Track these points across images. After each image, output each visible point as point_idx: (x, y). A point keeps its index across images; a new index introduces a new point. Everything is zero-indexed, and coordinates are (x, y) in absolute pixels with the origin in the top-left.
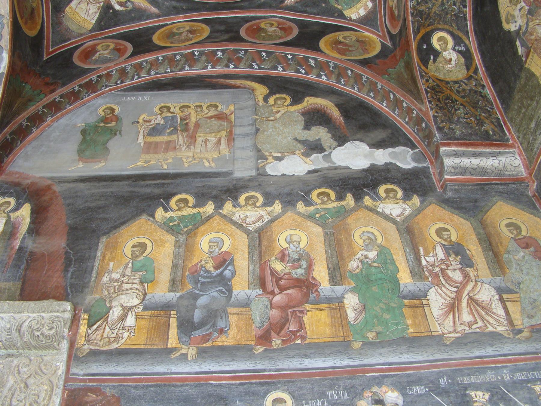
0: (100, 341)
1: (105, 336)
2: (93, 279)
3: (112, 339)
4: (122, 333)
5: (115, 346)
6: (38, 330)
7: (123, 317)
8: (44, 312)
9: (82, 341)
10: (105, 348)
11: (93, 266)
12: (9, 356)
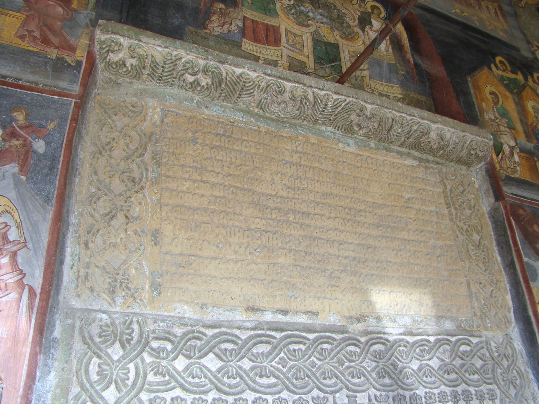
2: (479, 114)
6: (474, 150)
7: (512, 154)
8: (479, 136)
11: (473, 102)
12: (437, 163)
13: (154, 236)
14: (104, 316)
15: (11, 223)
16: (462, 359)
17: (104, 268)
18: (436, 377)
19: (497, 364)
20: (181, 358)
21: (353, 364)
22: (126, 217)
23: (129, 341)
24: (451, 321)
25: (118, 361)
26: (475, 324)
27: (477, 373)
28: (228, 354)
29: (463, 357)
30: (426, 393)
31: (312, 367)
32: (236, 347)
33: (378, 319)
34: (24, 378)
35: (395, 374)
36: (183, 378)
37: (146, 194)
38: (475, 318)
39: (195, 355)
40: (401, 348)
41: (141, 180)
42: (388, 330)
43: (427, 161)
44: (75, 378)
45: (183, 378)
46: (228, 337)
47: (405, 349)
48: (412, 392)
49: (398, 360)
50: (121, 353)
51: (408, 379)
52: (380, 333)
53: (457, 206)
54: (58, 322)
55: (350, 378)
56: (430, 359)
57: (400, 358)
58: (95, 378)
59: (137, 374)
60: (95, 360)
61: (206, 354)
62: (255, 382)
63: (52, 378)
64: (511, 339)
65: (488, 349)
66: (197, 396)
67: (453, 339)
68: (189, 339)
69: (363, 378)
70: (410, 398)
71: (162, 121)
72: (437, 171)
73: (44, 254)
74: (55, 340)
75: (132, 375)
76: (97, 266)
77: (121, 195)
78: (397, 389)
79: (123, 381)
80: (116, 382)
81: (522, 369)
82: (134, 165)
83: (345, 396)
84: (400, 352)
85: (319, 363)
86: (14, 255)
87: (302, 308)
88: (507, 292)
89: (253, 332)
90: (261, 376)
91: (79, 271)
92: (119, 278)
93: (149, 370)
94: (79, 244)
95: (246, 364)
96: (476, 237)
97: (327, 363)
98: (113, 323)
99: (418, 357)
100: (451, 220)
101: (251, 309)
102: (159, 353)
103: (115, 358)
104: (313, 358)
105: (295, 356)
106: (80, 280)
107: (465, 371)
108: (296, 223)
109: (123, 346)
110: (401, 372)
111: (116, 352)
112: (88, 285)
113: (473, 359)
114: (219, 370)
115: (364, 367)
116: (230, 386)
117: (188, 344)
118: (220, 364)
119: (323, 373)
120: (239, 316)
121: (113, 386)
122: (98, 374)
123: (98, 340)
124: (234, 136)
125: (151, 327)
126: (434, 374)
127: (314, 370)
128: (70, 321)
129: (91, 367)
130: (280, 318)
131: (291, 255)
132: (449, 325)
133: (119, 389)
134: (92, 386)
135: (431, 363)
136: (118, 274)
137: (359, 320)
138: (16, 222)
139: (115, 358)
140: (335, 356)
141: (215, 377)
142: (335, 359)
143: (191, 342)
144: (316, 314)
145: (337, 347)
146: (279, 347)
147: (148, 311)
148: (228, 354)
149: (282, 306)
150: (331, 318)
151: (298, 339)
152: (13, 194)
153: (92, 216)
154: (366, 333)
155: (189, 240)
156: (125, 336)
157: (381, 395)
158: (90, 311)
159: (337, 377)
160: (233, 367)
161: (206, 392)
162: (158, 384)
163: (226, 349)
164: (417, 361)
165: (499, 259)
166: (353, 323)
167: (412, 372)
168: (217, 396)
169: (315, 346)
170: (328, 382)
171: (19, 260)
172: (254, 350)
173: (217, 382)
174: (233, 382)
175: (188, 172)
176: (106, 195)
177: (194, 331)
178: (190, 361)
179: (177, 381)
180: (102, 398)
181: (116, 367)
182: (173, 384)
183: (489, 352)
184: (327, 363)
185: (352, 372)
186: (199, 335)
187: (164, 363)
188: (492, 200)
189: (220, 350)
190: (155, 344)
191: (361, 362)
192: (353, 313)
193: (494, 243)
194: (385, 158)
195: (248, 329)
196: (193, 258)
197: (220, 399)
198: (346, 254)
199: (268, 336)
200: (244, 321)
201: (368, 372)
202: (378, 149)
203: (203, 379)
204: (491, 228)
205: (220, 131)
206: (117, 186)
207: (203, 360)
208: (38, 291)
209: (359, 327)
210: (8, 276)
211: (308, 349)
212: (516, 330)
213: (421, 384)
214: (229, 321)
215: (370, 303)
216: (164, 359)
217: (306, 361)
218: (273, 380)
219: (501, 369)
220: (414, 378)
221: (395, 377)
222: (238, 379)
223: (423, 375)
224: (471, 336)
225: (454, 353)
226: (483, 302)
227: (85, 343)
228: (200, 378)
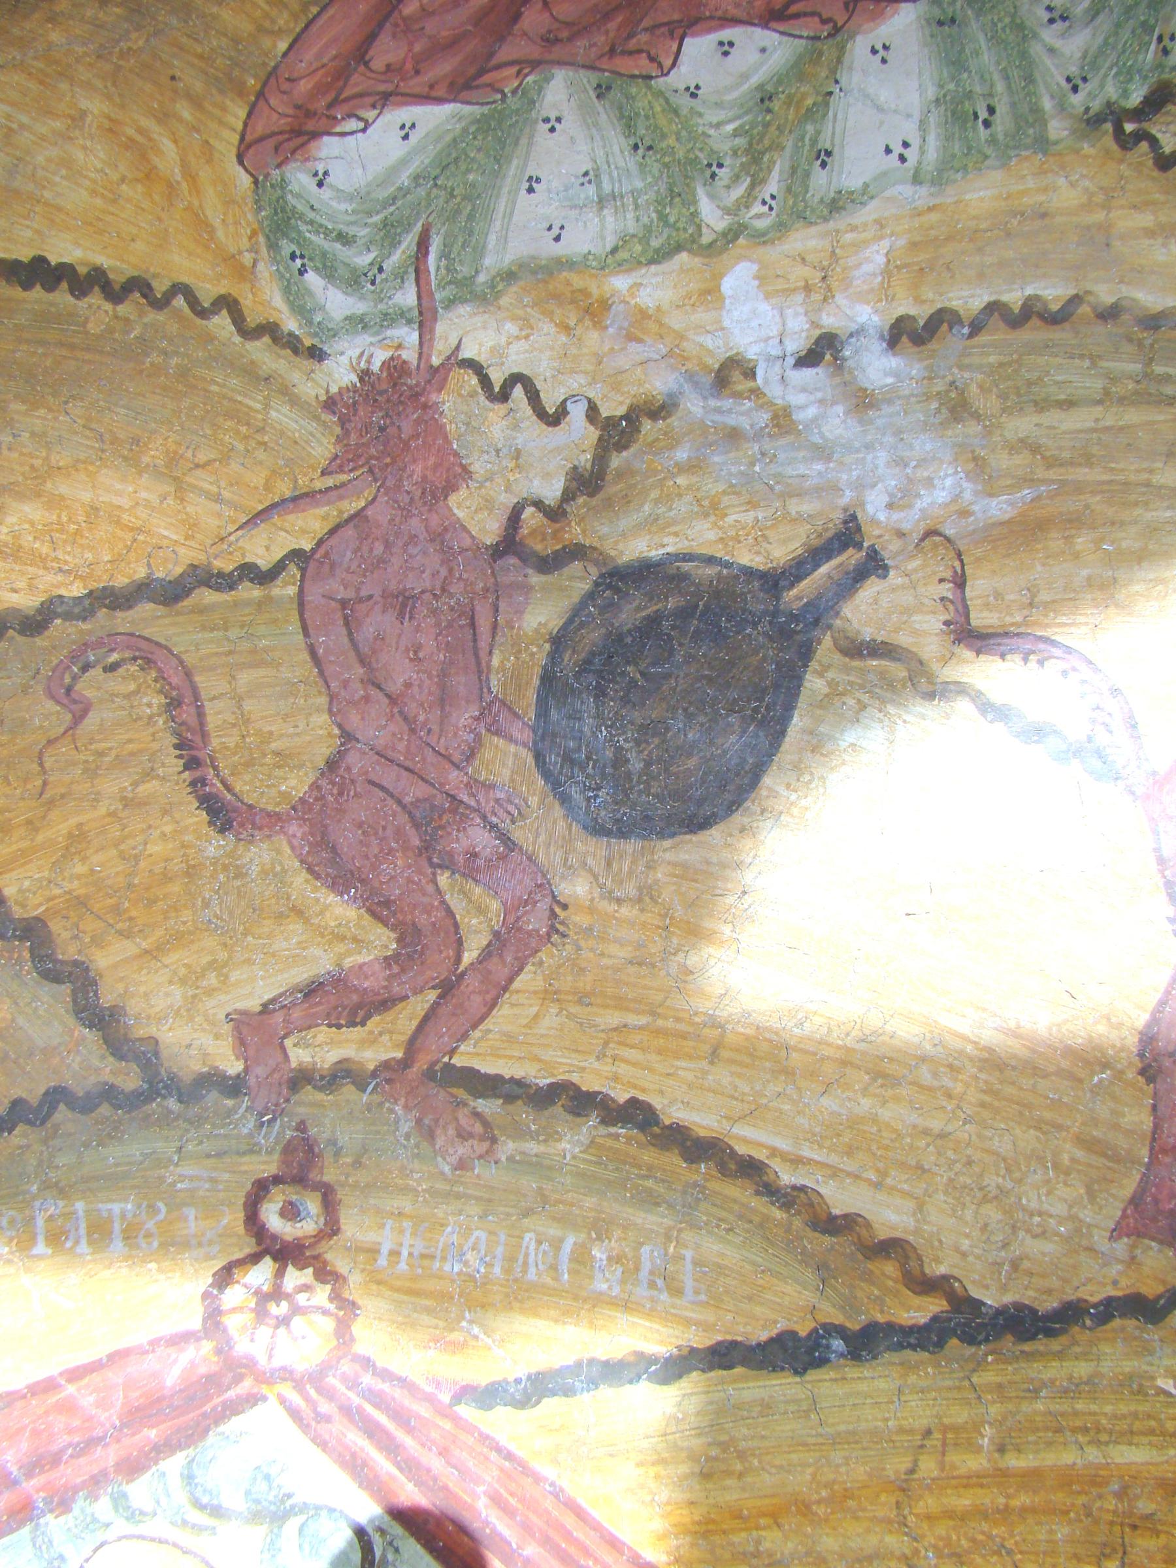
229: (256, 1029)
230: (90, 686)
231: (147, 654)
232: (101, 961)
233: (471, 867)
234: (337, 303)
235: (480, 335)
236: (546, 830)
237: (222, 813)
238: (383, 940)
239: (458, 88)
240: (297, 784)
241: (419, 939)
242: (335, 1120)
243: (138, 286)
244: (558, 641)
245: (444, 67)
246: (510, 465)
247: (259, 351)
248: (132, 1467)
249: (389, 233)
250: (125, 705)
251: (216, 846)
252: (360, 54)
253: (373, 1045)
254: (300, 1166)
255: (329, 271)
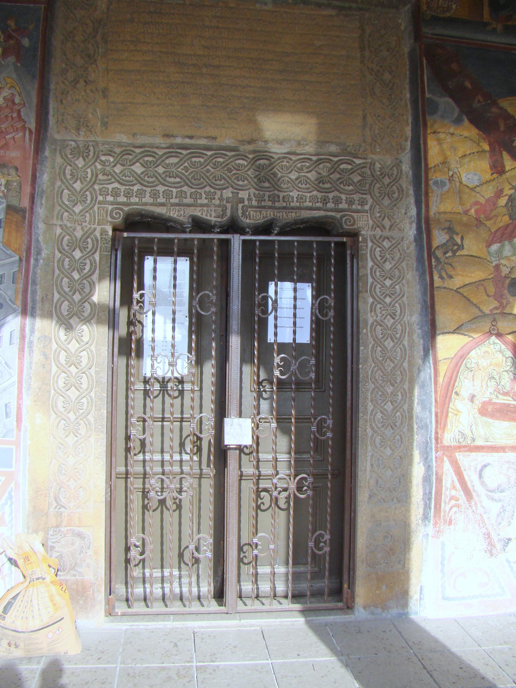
0: (437, 9)
1: (440, 5)
3: (445, 9)
4: (452, 5)
5: (448, 15)
9: (424, 7)
10: (442, 16)
13: (103, 92)
14: (73, 143)
15: (16, 93)
16: (340, 174)
17: (73, 115)
18: (310, 185)
19: (377, 180)
20: (119, 166)
21: (239, 172)
22: (85, 81)
23: (87, 156)
24: (337, 145)
25: (82, 168)
26: (362, 149)
27: (352, 185)
28: (148, 163)
29: (342, 172)
30: (298, 195)
31: (207, 173)
32: (154, 160)
33: (266, 142)
34: (30, 176)
35: (274, 180)
36: (119, 177)
37: (99, 65)
38: (363, 144)
39: (127, 164)
40: (284, 164)
41: (94, 55)
42: (273, 150)
43: (350, 9)
44: (58, 177)
45: (119, 177)
46: (150, 153)
47: (288, 164)
48: (286, 194)
49: (279, 171)
50: (83, 163)
51: (284, 184)
52: (266, 152)
53: (373, 49)
54: (47, 147)
55: (235, 181)
56: (307, 172)
57: (281, 170)
58: (69, 177)
59: (92, 175)
60: (69, 167)
61: (134, 163)
62: (165, 180)
63: (46, 177)
64: (401, 162)
65: (370, 168)
66: (127, 187)
67: (336, 159)
68: (124, 155)
69: (246, 182)
70: (283, 197)
71: (108, 9)
72: (358, 17)
73: (35, 109)
74: (46, 157)
75: (89, 176)
76: (68, 114)
77: (81, 67)
78: (274, 191)
79: (84, 178)
80: (80, 179)
81: (404, 186)
82: (90, 45)
83: (230, 192)
84: (282, 166)
85: (213, 170)
86: (19, 111)
87: (205, 135)
88: (408, 124)
89: (167, 150)
90: (170, 177)
91: (58, 118)
92: (82, 120)
93: (99, 172)
94: (57, 102)
95: (161, 170)
96: (387, 76)
97: (219, 171)
98: (78, 147)
99: (297, 170)
100: (362, 62)
101: (167, 136)
102: (105, 163)
103: (80, 166)
104: (208, 167)
105: (195, 165)
106: (59, 123)
107: (340, 183)
108: (208, 75)
109: (84, 159)
110: (279, 179)
111: (80, 162)
112: (64, 125)
113: (353, 175)
114: (142, 173)
115: (248, 175)
116: (148, 182)
117: (123, 157)
118: (143, 169)
119: (215, 177)
120: (159, 141)
121: (79, 182)
122: (71, 175)
123: (70, 156)
124: (163, 11)
125: (101, 148)
126: (308, 183)
127: (208, 174)
128: (54, 147)
129: (67, 171)
130: (187, 141)
131: (201, 98)
132: (333, 148)
133: (82, 183)
134: (67, 181)
135: (308, 175)
136: (81, 118)
137: (249, 143)
138: (18, 92)
139: (80, 166)
140: (225, 167)
141: (139, 176)
142: (226, 168)
143: (126, 157)
144: (215, 138)
145: (227, 160)
146: (184, 160)
147: (99, 139)
148: (148, 163)
149: (189, 133)
150: (228, 142)
151: (198, 155)
152: (14, 76)
153: (64, 83)
154: (254, 152)
155: (126, 93)
156: (85, 154)
157: (259, 193)
158: (64, 141)
159: (225, 179)
160: (151, 171)
161: (133, 185)
162: (104, 180)
163: (147, 161)
164: (296, 173)
165: (408, 95)
166: (244, 145)
167: (289, 180)
168: (140, 188)
169: (210, 159)
170: (218, 182)
171: (22, 114)
172: (167, 161)
173: (140, 180)
174: (151, 180)
175: (126, 45)
176: (71, 68)
177: (127, 150)
178: (124, 167)
179: (115, 179)
180: (73, 187)
181: (80, 171)
182: (113, 180)
183: (371, 171)
184: (219, 171)
185: (238, 177)
186: (130, 152)
187: (108, 168)
188: (412, 41)
189: (144, 161)
190: (103, 158)
191: (247, 171)
192: (245, 138)
193: (407, 81)
194: (302, 11)
195: (163, 148)
196: (129, 104)
197: (142, 189)
198: (247, 95)
199: (177, 152)
200: (161, 144)
201: (251, 178)
202: (296, 4)
203: (131, 178)
204: (408, 67)
205: (152, 9)
206: (79, 61)
207: (132, 167)
208: (34, 130)
209: (250, 147)
210: (17, 123)
211: (206, 161)
212: (409, 155)
213: (295, 188)
214: (151, 144)
215: (259, 130)
216: (107, 166)
217: (202, 169)
218: (178, 180)
219: (379, 184)
220: (289, 185)
221: (273, 183)
222: (154, 179)
223: (299, 183)
224: (354, 158)
225: (334, 169)
226: (377, 132)
227: (63, 158)
228: (130, 177)
229: (491, 311)
230: (479, 287)
231: (483, 285)
232: (480, 306)
233: (504, 299)
234: (493, 259)
235: (503, 262)
236: (508, 296)
237: (488, 296)
238: (499, 304)
239: (499, 242)
240: (493, 294)
241: (501, 304)
242: (497, 316)
243: (479, 257)
244: (509, 283)
245: (498, 241)
246: (505, 271)
247: (488, 263)
248: (485, 342)
249: (496, 254)
250: (481, 288)
251: (488, 298)
252: (493, 239)
253: (498, 311)
254: (494, 320)
255: (493, 257)
